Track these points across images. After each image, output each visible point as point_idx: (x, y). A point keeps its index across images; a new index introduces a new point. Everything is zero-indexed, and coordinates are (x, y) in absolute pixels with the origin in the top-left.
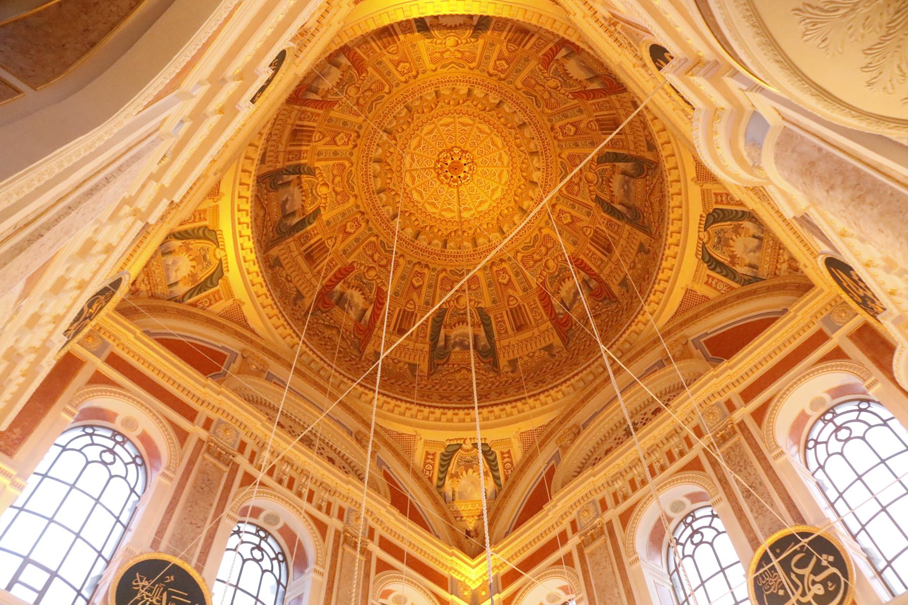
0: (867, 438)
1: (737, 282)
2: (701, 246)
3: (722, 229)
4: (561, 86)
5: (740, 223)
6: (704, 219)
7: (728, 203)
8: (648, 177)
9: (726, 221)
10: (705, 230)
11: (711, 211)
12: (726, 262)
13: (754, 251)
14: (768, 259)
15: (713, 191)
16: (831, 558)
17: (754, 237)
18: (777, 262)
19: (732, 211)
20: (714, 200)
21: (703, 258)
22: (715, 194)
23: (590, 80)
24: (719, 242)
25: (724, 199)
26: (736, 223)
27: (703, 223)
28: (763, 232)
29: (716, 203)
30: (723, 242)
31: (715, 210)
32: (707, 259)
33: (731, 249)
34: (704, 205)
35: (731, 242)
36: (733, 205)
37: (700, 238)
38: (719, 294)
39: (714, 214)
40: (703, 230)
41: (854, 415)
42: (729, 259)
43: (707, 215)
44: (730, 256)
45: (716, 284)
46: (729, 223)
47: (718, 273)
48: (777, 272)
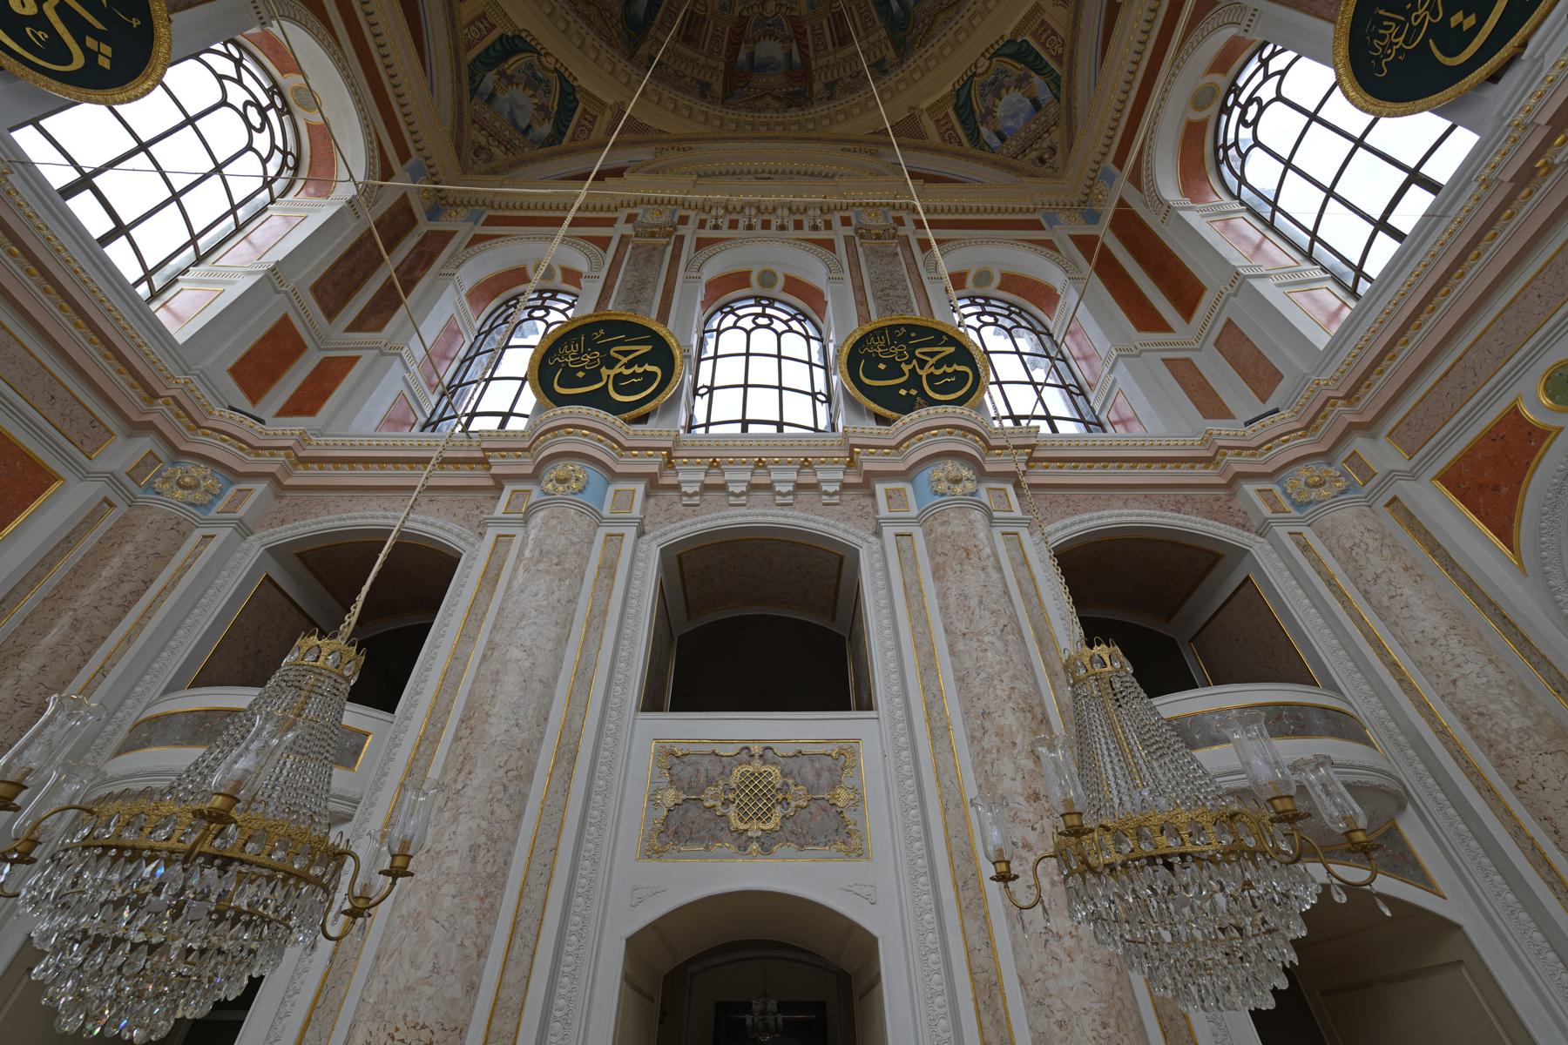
0: (250, 154)
1: (475, 60)
2: (538, 47)
3: (550, 92)
4: (762, 14)
5: (552, 121)
6: (571, 79)
7: (579, 124)
8: (620, 26)
9: (558, 105)
10: (556, 70)
11: (578, 97)
12: (506, 66)
13: (511, 113)
14: (497, 124)
15: (600, 117)
16: (105, 63)
17: (529, 127)
18: (491, 135)
19: (570, 121)
20: (589, 109)
21: (520, 37)
22: (595, 117)
23: (751, 55)
24: (534, 75)
25: (587, 123)
26: (552, 115)
27: (567, 75)
28: (532, 141)
29: (585, 109)
30: (534, 82)
31: (576, 102)
32: (516, 40)
33: (521, 86)
34: (587, 93)
35: (531, 92)
36: (576, 128)
37: (547, 54)
38: (464, 23)
39: (571, 98)
40: (558, 66)
41: (279, 142)
42: (509, 72)
43: (573, 87)
44: (513, 76)
45: (480, 30)
46: (556, 108)
47: (494, 43)
48: (476, 126)
